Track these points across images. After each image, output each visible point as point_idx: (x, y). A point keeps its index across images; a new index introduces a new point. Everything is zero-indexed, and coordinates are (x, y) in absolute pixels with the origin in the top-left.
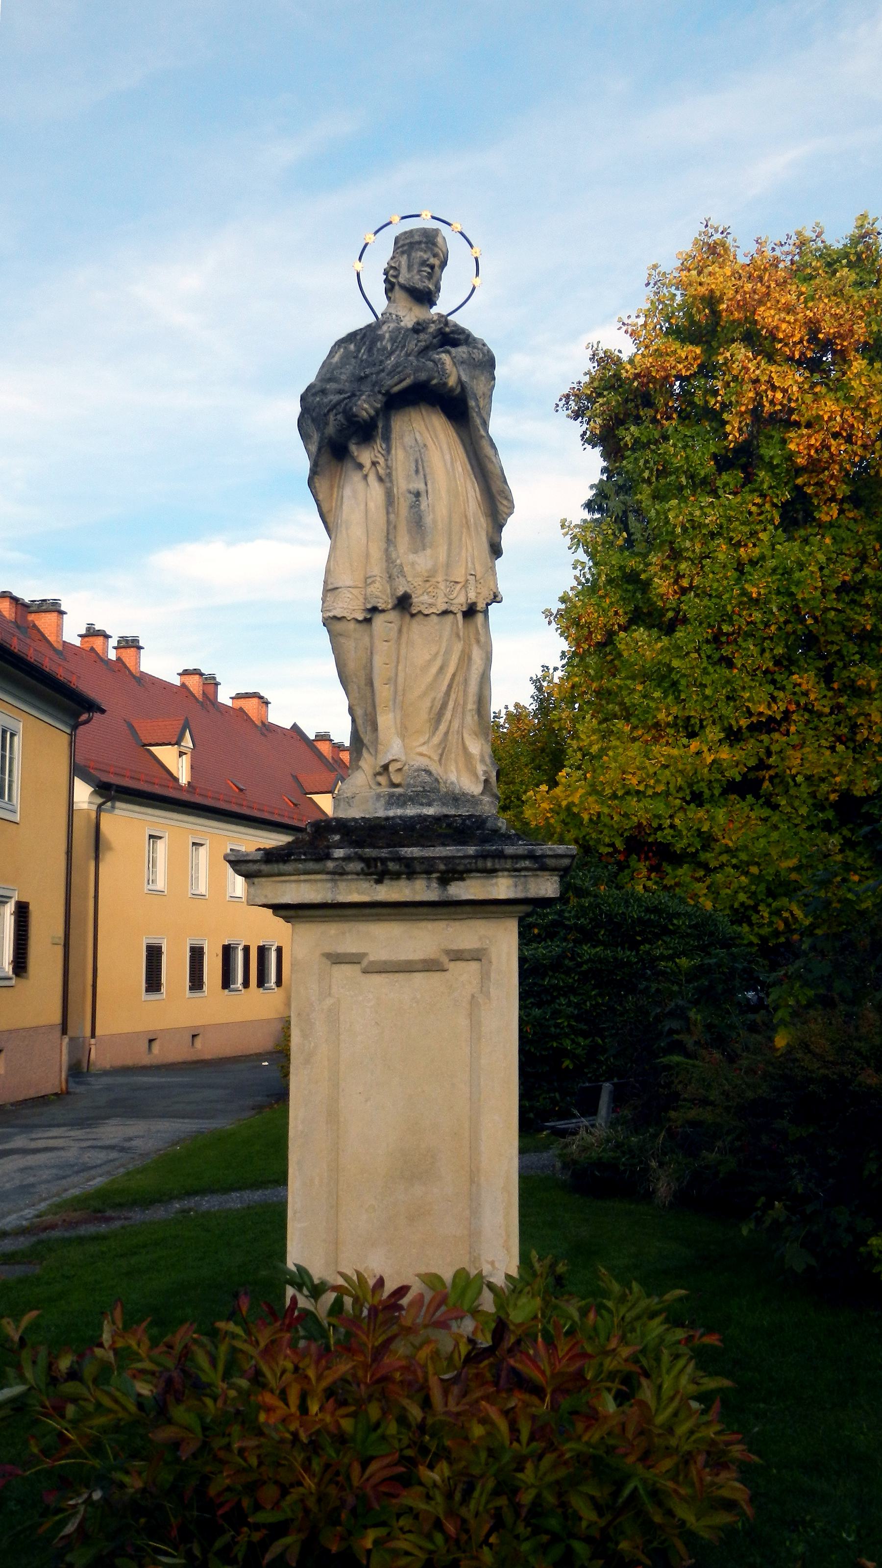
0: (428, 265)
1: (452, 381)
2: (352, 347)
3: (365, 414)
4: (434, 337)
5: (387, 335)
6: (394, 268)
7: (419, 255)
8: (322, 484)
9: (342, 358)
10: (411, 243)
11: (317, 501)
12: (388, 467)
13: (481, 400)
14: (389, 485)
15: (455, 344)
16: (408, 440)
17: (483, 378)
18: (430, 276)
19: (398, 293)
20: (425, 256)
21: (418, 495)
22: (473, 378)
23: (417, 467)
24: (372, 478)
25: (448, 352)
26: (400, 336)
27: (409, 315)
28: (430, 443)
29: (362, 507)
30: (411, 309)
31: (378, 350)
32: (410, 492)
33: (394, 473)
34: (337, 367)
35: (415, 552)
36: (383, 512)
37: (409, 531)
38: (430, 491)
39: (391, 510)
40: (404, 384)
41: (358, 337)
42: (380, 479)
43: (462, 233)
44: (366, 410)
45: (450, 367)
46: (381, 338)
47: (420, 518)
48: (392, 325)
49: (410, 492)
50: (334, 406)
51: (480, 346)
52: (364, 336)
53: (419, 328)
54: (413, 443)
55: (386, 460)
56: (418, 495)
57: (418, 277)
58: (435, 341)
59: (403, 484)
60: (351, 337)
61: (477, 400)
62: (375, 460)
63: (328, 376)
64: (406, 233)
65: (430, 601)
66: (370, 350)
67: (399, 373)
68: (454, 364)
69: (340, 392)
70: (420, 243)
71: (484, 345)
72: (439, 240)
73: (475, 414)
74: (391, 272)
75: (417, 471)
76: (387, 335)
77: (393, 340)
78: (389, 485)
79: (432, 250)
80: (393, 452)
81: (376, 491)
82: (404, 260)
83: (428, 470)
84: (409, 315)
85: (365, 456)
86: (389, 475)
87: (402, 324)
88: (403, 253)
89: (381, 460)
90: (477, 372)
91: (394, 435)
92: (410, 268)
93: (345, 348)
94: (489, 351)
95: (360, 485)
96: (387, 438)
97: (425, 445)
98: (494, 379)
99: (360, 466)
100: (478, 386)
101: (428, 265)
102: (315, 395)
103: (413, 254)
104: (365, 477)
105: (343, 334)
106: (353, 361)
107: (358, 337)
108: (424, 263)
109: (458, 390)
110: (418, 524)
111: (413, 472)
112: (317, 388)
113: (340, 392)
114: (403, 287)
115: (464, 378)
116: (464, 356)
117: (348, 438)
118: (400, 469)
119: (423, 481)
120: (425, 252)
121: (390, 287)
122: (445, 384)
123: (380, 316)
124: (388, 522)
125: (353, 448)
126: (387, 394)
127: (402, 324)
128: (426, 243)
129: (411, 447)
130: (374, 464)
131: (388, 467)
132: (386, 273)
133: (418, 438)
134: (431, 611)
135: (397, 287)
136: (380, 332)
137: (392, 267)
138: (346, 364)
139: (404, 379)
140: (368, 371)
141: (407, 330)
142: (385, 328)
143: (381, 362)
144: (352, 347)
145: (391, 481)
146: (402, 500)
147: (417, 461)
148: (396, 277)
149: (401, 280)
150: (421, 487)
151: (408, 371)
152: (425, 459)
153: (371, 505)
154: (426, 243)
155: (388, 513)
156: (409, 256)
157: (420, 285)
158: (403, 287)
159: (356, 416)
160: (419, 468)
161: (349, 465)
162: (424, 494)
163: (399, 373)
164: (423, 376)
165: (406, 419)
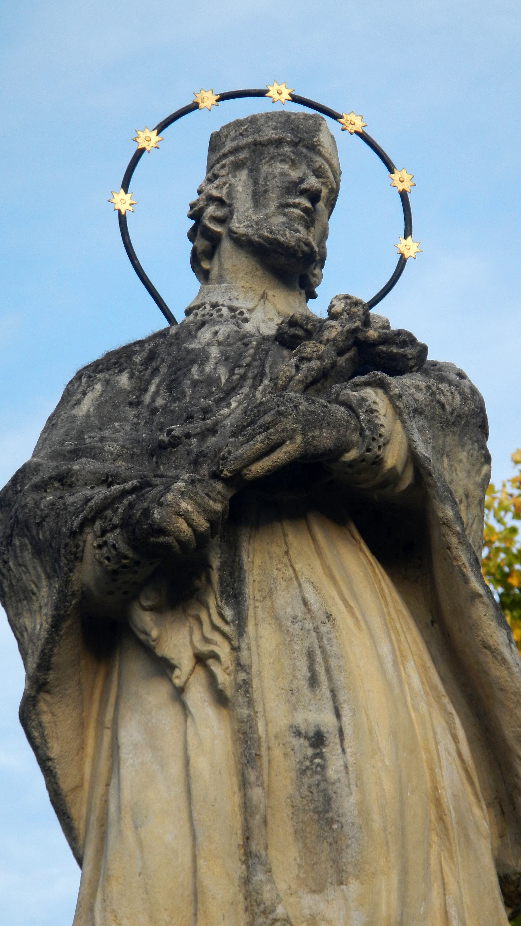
0: (303, 193)
1: (393, 457)
2: (124, 380)
4: (340, 353)
5: (214, 352)
6: (220, 202)
7: (279, 170)
8: (59, 717)
9: (100, 405)
10: (255, 144)
11: (45, 763)
12: (240, 666)
13: (462, 508)
14: (245, 712)
15: (397, 366)
16: (286, 601)
17: (463, 455)
18: (310, 218)
19: (229, 257)
20: (295, 175)
21: (318, 740)
22: (441, 452)
23: (311, 669)
24: (198, 696)
26: (247, 357)
27: (264, 310)
28: (338, 609)
29: (175, 769)
30: (264, 297)
31: (195, 384)
32: (298, 733)
33: (255, 683)
34: (87, 426)
35: (318, 889)
36: (229, 783)
37: (299, 834)
38: (348, 731)
39: (252, 777)
41: (137, 359)
42: (221, 699)
43: (363, 136)
45: (390, 426)
46: (200, 357)
47: (328, 800)
48: (224, 330)
49: (298, 733)
50: (99, 512)
51: (453, 377)
52: (152, 356)
53: (294, 334)
54: (299, 610)
55: (235, 649)
56: (318, 740)
57: (281, 219)
58: (341, 361)
59: (276, 712)
60: (116, 360)
61: (454, 505)
62: (205, 648)
63: (70, 445)
64: (238, 124)
66: (172, 386)
67: (266, 427)
68: (398, 413)
69: (107, 481)
70: (279, 143)
71: (461, 375)
72: (323, 138)
73: (454, 541)
74: (211, 210)
75: (313, 681)
76: (214, 352)
77: (231, 361)
78: (245, 712)
79: (310, 163)
80: (250, 628)
81: (211, 728)
82: (241, 182)
83: (340, 679)
84: (264, 310)
85: (178, 642)
86: (245, 687)
87: (248, 327)
88: (237, 166)
89: (223, 649)
91: (251, 590)
92: (258, 198)
93: (107, 382)
94: (474, 391)
95: (167, 717)
96: (234, 595)
97: (329, 616)
98: (487, 459)
99: (164, 667)
100: (453, 473)
101: (303, 193)
102: (41, 487)
103: (265, 168)
104: (179, 694)
105: (96, 354)
106: (131, 412)
107: (137, 359)
108: (293, 188)
109: (408, 479)
110: (321, 813)
111: (304, 684)
112: (45, 474)
113: (107, 481)
114: (242, 243)
115: (422, 449)
117: (132, 596)
118: (268, 673)
119: (329, 705)
120: (294, 164)
121: (206, 244)
122: (378, 461)
123: (180, 317)
124: (247, 808)
125: (146, 621)
126: (236, 481)
127: (248, 327)
128: (294, 144)
129: (294, 620)
130: (201, 660)
131: (240, 666)
132: (196, 214)
135: (226, 245)
136: (194, 345)
137: (211, 199)
138: (111, 420)
139: (279, 444)
140: (178, 430)
141: (265, 338)
142: (206, 335)
143: (206, 411)
144: (124, 380)
145: (250, 703)
146: (277, 753)
147: (310, 655)
148: (221, 221)
149: (239, 226)
150: (326, 720)
152: (333, 650)
153: (201, 764)
155: (244, 784)
156: (254, 172)
157: (288, 237)
158: (242, 243)
159: (162, 531)
160: (318, 672)
161: (134, 666)
162: (333, 740)
163: (266, 427)
165: (277, 550)
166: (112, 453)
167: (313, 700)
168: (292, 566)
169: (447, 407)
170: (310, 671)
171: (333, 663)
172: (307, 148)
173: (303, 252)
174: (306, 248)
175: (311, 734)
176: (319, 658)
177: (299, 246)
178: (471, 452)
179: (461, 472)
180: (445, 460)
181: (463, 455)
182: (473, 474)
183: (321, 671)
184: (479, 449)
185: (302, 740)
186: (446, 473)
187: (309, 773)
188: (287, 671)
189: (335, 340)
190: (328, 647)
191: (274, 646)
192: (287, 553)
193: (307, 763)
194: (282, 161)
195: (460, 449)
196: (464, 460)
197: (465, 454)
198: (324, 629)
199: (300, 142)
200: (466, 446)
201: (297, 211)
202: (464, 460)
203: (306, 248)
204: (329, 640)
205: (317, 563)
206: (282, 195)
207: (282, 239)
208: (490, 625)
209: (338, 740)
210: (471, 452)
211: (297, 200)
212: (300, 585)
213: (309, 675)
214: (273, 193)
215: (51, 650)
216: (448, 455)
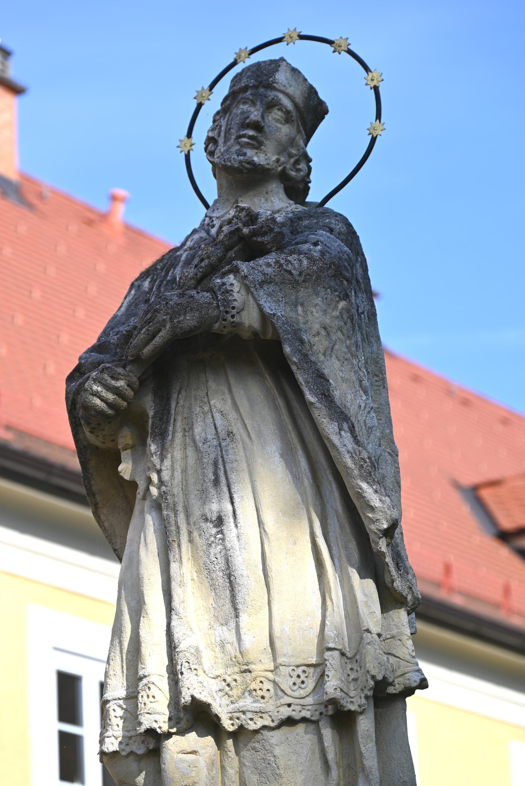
3: (97, 402)
17: (318, 301)
25: (235, 271)
40: (158, 340)
44: (96, 394)
65: (256, 706)
90: (303, 293)
97: (230, 434)
116: (269, 270)
133: (219, 423)
134: (260, 723)
147: (215, 464)
151: (161, 317)
154: (255, 87)
164: (189, 320)
166: (113, 344)
167: (215, 495)
168: (209, 403)
169: (294, 272)
170: (214, 475)
171: (228, 466)
172: (264, 87)
173: (246, 169)
174: (248, 166)
175: (214, 519)
176: (221, 466)
177: (242, 166)
178: (325, 296)
179: (317, 312)
180: (300, 309)
181: (318, 301)
182: (329, 311)
183: (222, 474)
184: (331, 292)
185: (208, 524)
186: (300, 318)
187: (213, 545)
188: (201, 478)
189: (222, 242)
190: (225, 456)
191: (194, 462)
192: (207, 395)
193: (212, 539)
194: (245, 103)
195: (315, 297)
196: (320, 303)
197: (320, 299)
198: (223, 444)
199: (259, 84)
200: (320, 293)
201: (245, 140)
202: (320, 303)
203: (248, 166)
204: (227, 451)
205: (228, 397)
206: (239, 130)
207: (229, 164)
208: (323, 421)
209: (232, 520)
210: (325, 296)
211: (244, 132)
212: (213, 417)
213: (213, 478)
214: (233, 129)
215: (89, 483)
216: (302, 305)
